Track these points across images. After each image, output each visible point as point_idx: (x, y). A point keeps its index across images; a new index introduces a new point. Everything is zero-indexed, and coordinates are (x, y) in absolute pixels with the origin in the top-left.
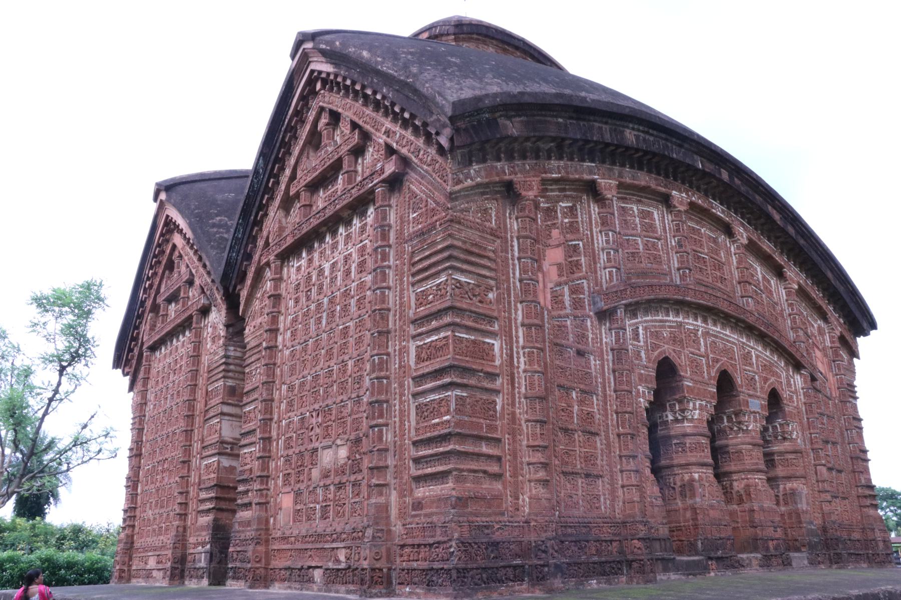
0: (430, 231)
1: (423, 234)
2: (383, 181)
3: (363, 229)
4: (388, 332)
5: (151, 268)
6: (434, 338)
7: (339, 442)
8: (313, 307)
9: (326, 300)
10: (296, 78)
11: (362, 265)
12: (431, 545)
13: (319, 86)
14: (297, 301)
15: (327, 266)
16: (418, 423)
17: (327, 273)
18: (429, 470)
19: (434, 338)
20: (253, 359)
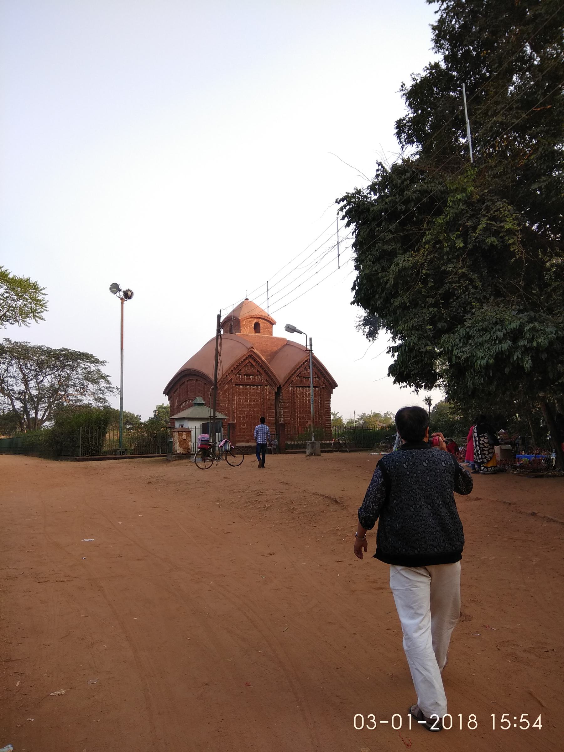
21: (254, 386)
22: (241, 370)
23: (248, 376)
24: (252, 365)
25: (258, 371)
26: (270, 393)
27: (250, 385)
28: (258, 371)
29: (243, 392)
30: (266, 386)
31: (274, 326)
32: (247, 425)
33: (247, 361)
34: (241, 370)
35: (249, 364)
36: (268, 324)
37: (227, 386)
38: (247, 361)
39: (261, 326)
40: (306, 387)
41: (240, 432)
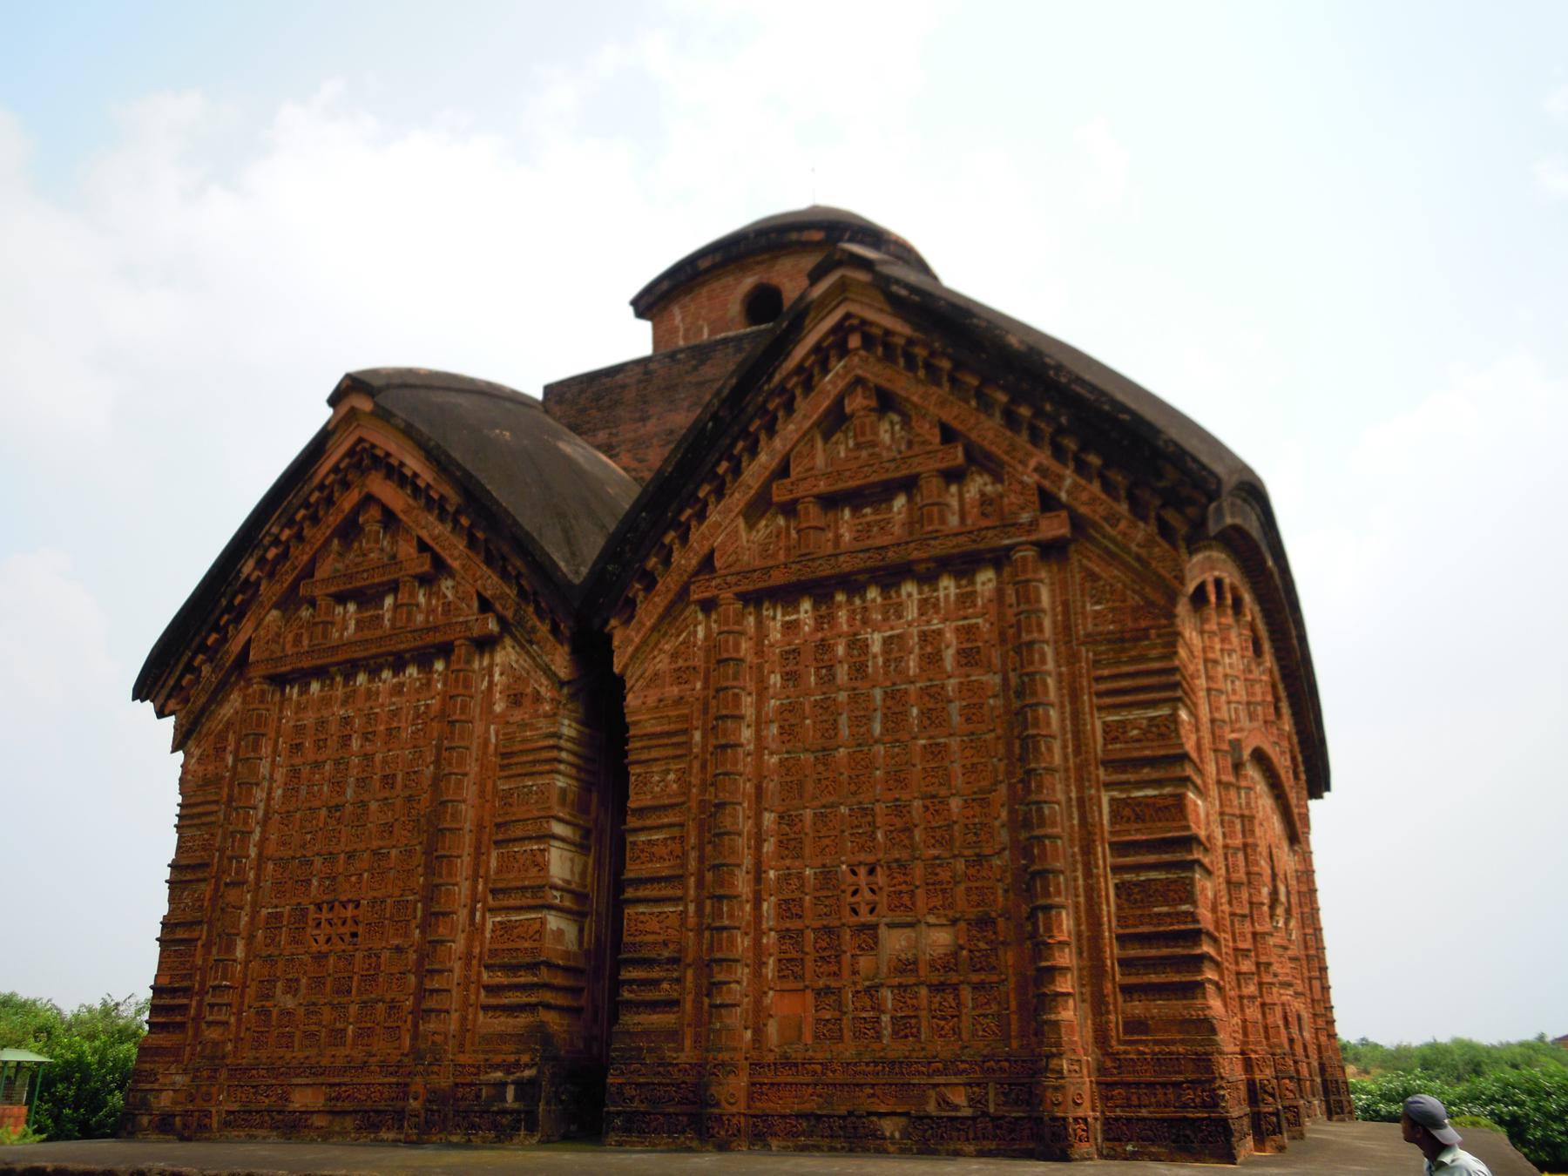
0: (1137, 639)
1: (1122, 640)
2: (1033, 543)
3: (966, 599)
4: (1055, 770)
5: (290, 523)
6: (1150, 792)
7: (931, 919)
8: (842, 697)
9: (878, 694)
10: (812, 314)
11: (968, 657)
12: (1178, 1085)
13: (854, 341)
14: (789, 677)
15: (876, 642)
16: (1119, 907)
17: (876, 648)
18: (1154, 978)
19: (1150, 792)
20: (654, 754)
23: (367, 597)
25: (423, 547)
26: (516, 700)
29: (322, 723)
30: (485, 644)
35: (375, 512)
38: (348, 502)
40: (852, 584)
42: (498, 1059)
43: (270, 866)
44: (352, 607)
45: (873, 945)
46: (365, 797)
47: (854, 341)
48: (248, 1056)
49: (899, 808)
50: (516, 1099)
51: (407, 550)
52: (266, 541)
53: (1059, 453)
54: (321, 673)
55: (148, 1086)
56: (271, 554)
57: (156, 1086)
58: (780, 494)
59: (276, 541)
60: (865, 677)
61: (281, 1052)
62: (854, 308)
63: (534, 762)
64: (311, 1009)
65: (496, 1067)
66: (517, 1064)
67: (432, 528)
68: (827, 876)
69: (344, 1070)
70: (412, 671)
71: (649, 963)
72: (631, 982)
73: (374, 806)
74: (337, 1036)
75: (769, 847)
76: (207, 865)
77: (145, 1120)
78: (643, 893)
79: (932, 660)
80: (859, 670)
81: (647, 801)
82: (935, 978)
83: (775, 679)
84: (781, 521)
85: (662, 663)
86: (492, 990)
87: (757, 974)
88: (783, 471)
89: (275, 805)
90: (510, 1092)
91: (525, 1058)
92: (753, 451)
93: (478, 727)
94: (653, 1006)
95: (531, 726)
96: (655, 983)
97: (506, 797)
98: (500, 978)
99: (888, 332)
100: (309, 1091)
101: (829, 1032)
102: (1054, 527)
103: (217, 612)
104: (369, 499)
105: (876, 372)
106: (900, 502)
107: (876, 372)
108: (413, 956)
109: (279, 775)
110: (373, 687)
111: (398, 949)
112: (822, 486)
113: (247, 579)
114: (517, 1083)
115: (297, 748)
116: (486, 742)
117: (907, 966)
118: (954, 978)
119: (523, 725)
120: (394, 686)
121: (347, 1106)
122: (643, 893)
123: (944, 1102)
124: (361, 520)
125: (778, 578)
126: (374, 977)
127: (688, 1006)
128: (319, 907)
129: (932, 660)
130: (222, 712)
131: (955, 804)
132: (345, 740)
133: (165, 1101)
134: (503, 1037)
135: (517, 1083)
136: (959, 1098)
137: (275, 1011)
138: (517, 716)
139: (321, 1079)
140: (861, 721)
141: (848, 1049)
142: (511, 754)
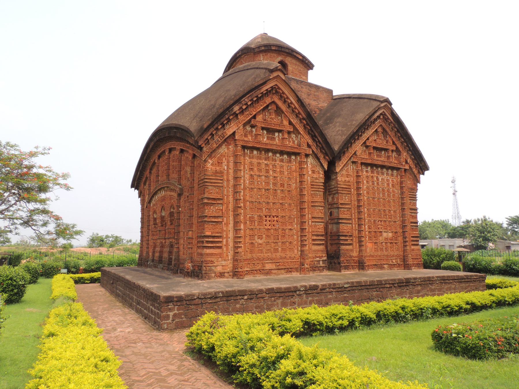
13: (381, 117)
14: (367, 182)
15: (380, 178)
21: (282, 153)
22: (254, 117)
24: (279, 111)
25: (290, 123)
26: (313, 172)
27: (275, 152)
28: (290, 123)
30: (307, 156)
31: (310, 72)
32: (268, 236)
33: (268, 100)
34: (254, 117)
35: (273, 107)
36: (301, 67)
37: (224, 150)
38: (268, 100)
39: (290, 68)
40: (377, 166)
41: (251, 252)
42: (318, 255)
43: (248, 203)
44: (265, 132)
45: (381, 235)
46: (275, 188)
47: (381, 117)
48: (249, 256)
49: (384, 211)
50: (323, 263)
51: (286, 123)
52: (243, 102)
53: (408, 153)
54: (258, 149)
55: (212, 265)
56: (244, 107)
57: (215, 265)
58: (368, 144)
59: (246, 104)
60: (378, 185)
61: (260, 254)
62: (385, 111)
63: (319, 188)
64: (268, 243)
65: (317, 257)
66: (322, 256)
67: (294, 121)
68: (375, 221)
69: (281, 258)
70: (285, 156)
71: (346, 236)
72: (342, 240)
73: (279, 191)
74: (276, 250)
75: (366, 215)
76: (222, 199)
77: (213, 275)
78: (343, 221)
79: (388, 185)
80: (378, 184)
81: (343, 202)
82: (390, 241)
83: (365, 182)
84: (365, 148)
85: (344, 172)
86: (313, 240)
87: (365, 239)
88: (368, 139)
89: (247, 185)
90: (321, 262)
91: (324, 255)
92: (364, 132)
93: (306, 176)
94: (347, 244)
95: (318, 180)
96: (347, 240)
97: (312, 194)
98: (315, 238)
99: (388, 118)
100: (270, 264)
101: (376, 250)
102: (407, 167)
103: (224, 119)
104: (273, 102)
105: (384, 125)
106: (383, 152)
107: (384, 125)
108: (295, 231)
109: (247, 176)
110: (274, 157)
111: (291, 229)
112: (374, 145)
113: (235, 113)
114: (322, 261)
115: (252, 169)
116: (308, 180)
117: (386, 239)
118: (392, 241)
119: (316, 179)
120: (280, 159)
121: (282, 267)
122: (343, 221)
123: (392, 262)
124: (270, 108)
125: (369, 162)
126: (284, 236)
127: (354, 245)
128: (266, 217)
129: (388, 185)
130: (220, 151)
131: (392, 211)
132: (267, 171)
133: (219, 269)
134: (318, 251)
135: (322, 261)
136: (394, 261)
137: (256, 244)
138: (315, 176)
139: (274, 261)
140: (379, 194)
141: (379, 253)
142: (314, 185)
